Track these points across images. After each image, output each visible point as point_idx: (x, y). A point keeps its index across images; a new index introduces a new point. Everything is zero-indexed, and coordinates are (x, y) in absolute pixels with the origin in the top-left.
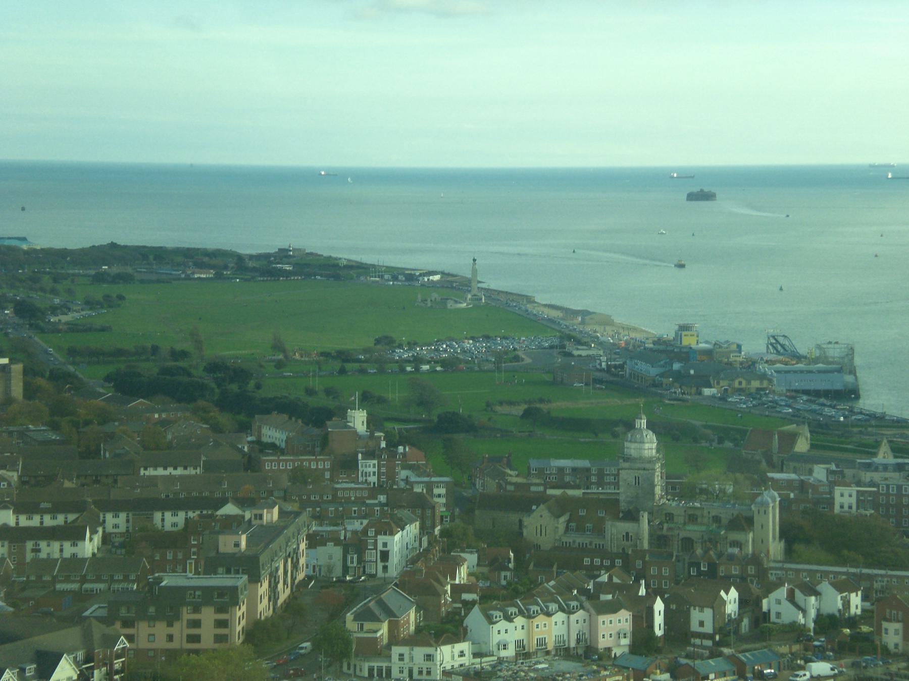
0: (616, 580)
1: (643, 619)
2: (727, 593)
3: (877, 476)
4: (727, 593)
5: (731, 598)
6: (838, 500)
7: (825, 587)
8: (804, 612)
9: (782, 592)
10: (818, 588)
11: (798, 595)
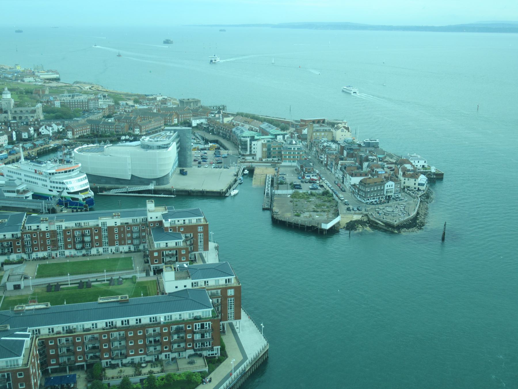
0: (3, 128)
1: (10, 138)
2: (31, 128)
3: (65, 98)
4: (31, 128)
5: (32, 130)
6: (56, 104)
7: (54, 125)
8: (49, 131)
9: (44, 127)
10: (52, 125)
11: (47, 127)
